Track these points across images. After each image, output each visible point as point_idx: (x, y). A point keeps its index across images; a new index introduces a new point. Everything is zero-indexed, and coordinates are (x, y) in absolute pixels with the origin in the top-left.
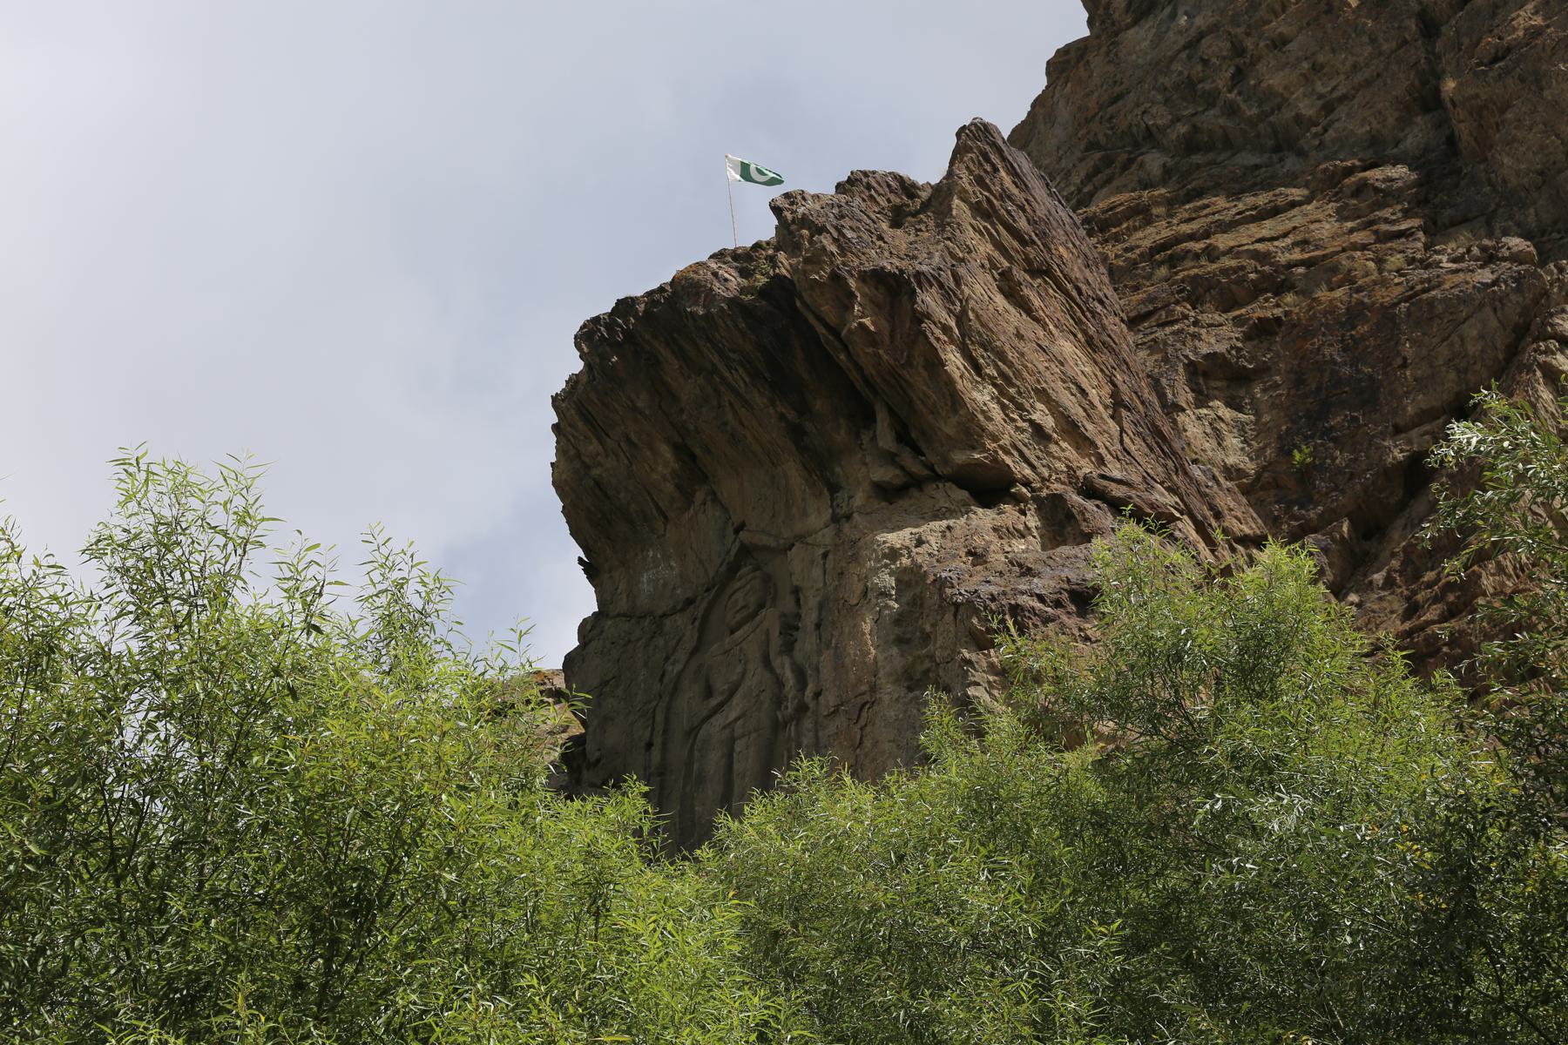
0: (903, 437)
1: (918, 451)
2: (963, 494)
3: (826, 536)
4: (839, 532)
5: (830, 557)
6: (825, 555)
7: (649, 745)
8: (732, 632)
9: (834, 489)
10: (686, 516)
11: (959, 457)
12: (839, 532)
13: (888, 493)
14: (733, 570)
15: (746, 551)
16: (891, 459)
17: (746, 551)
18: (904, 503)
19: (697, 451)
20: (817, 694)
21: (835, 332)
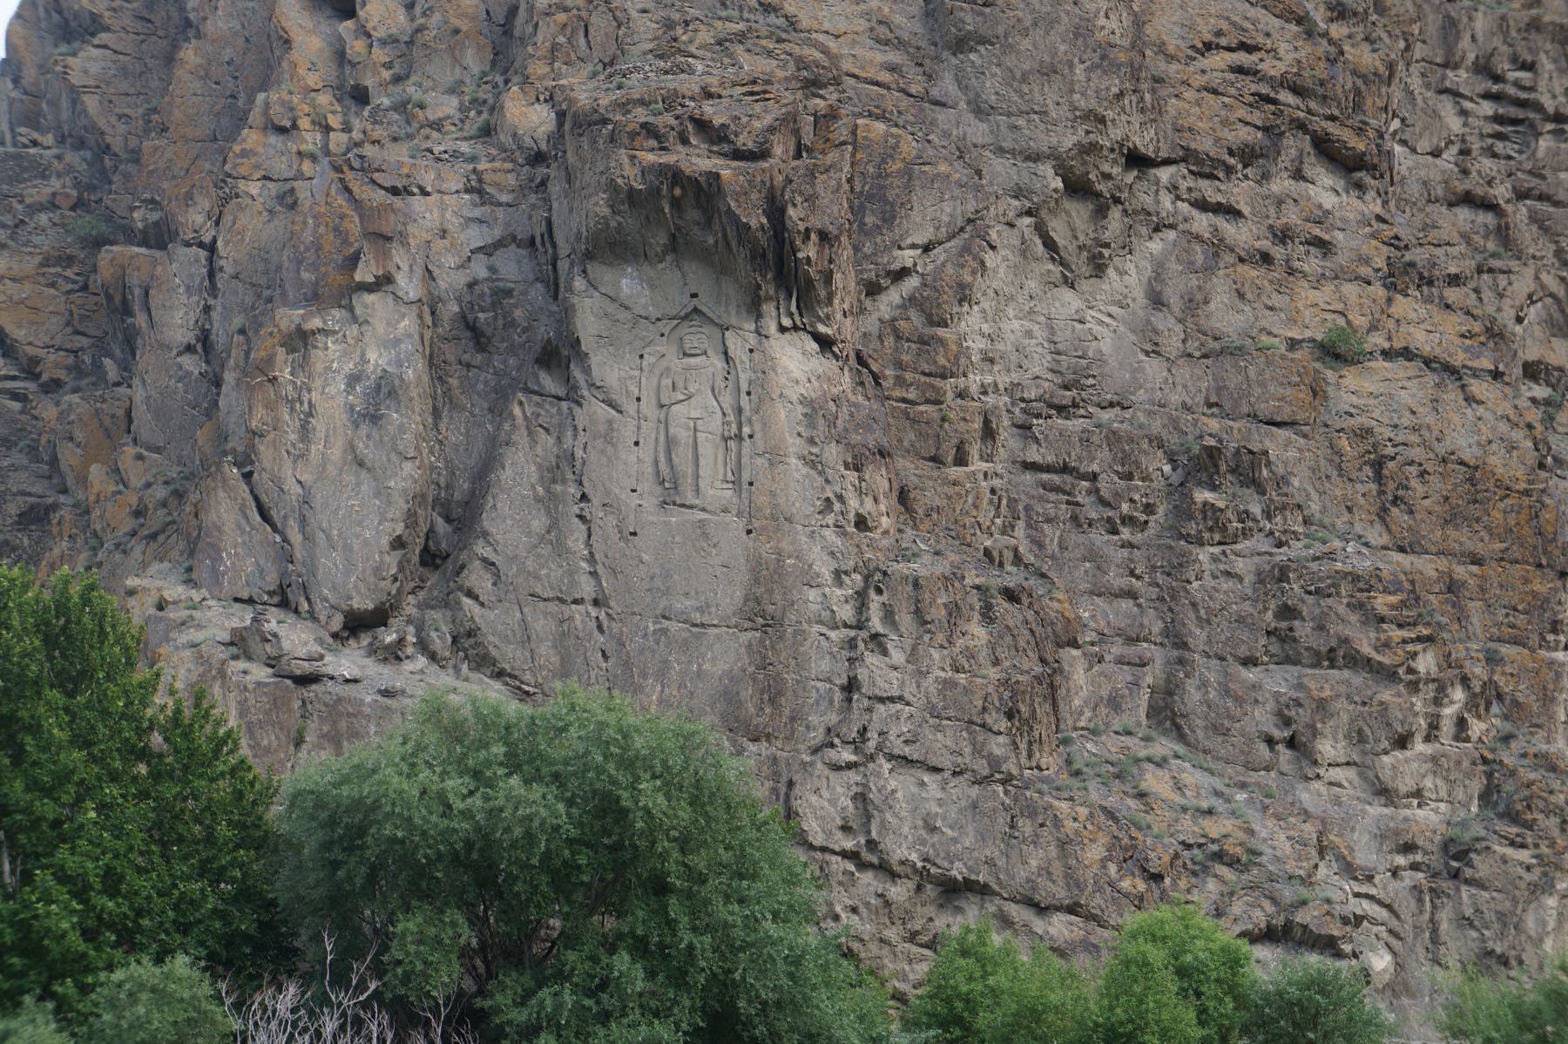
0: (798, 307)
1: (801, 315)
2: (816, 346)
3: (752, 339)
4: (760, 343)
5: (755, 355)
6: (751, 351)
7: (638, 399)
8: (685, 354)
9: (759, 316)
10: (661, 266)
11: (822, 329)
12: (760, 343)
13: (783, 329)
14: (684, 318)
15: (696, 310)
16: (791, 315)
17: (696, 310)
18: (787, 335)
19: (680, 241)
20: (751, 437)
21: (795, 251)
